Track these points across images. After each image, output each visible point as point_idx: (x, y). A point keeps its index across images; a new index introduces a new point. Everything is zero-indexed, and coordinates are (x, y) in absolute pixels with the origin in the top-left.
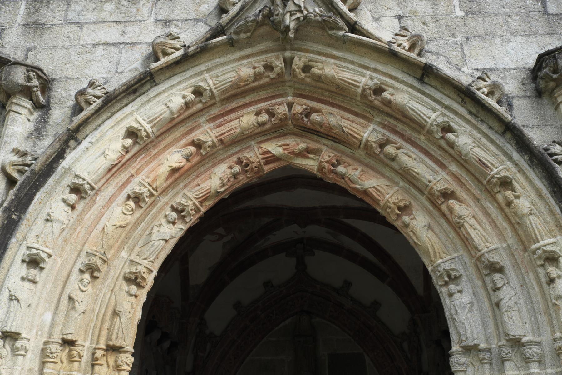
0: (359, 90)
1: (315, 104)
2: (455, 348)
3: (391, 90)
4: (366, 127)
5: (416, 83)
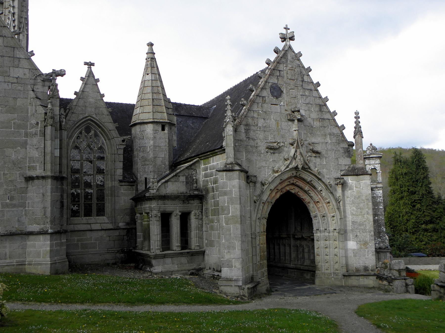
0: (308, 181)
1: (298, 181)
2: (314, 229)
3: (313, 182)
4: (306, 187)
5: (318, 181)
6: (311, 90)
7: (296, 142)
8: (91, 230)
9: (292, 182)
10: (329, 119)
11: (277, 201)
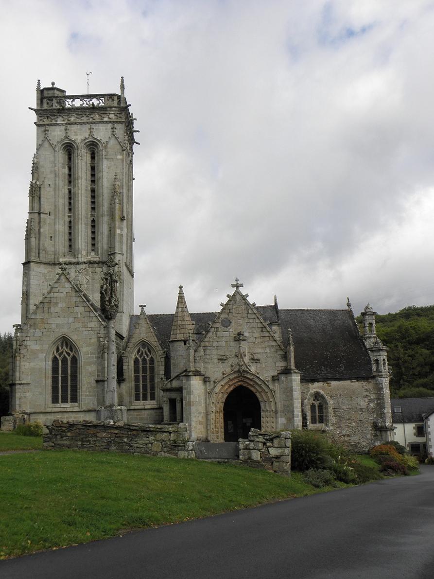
6: (254, 318)
7: (240, 355)
8: (145, 409)
9: (240, 379)
10: (269, 337)
11: (232, 392)
